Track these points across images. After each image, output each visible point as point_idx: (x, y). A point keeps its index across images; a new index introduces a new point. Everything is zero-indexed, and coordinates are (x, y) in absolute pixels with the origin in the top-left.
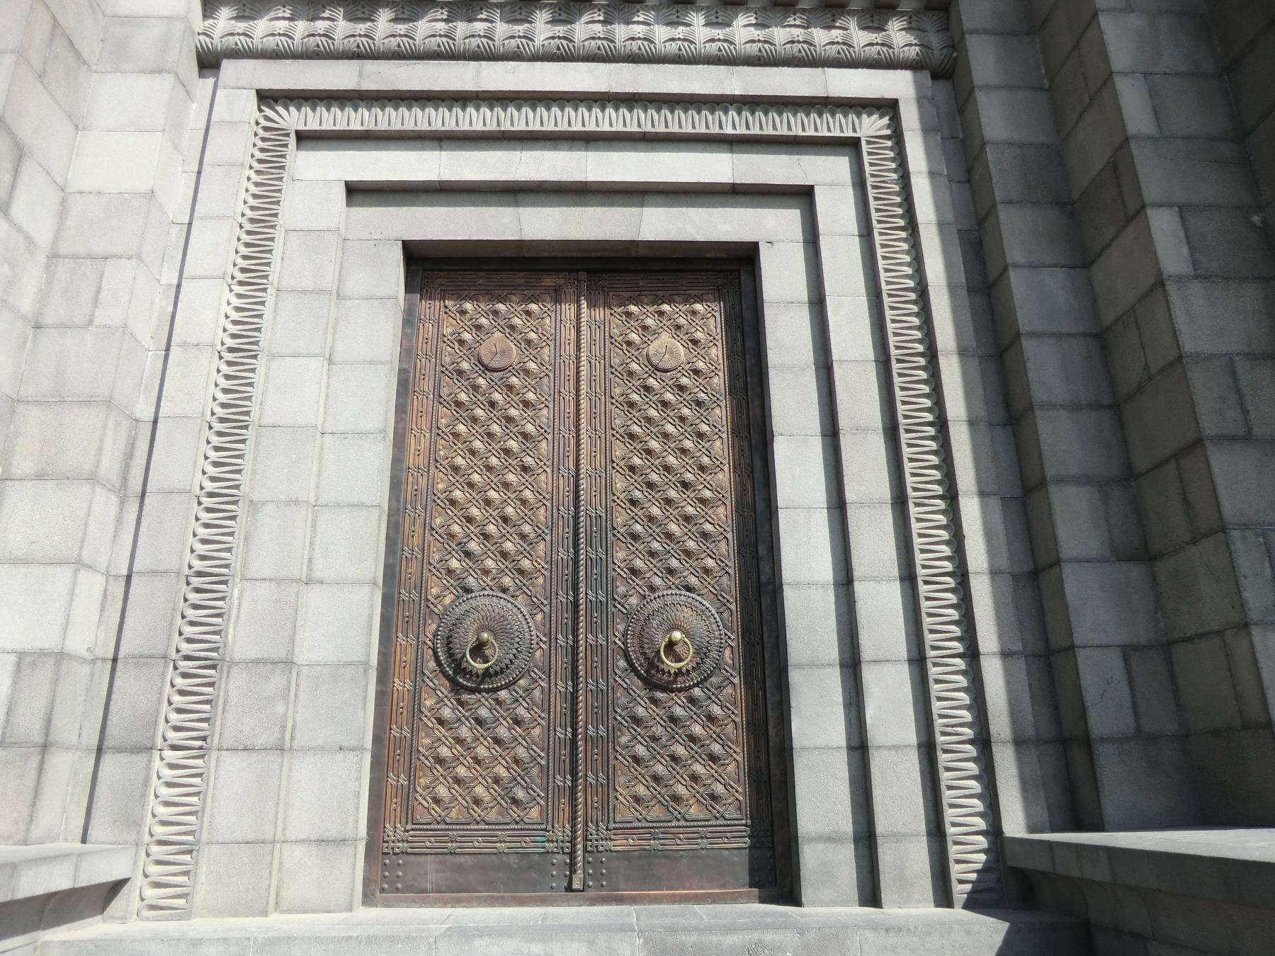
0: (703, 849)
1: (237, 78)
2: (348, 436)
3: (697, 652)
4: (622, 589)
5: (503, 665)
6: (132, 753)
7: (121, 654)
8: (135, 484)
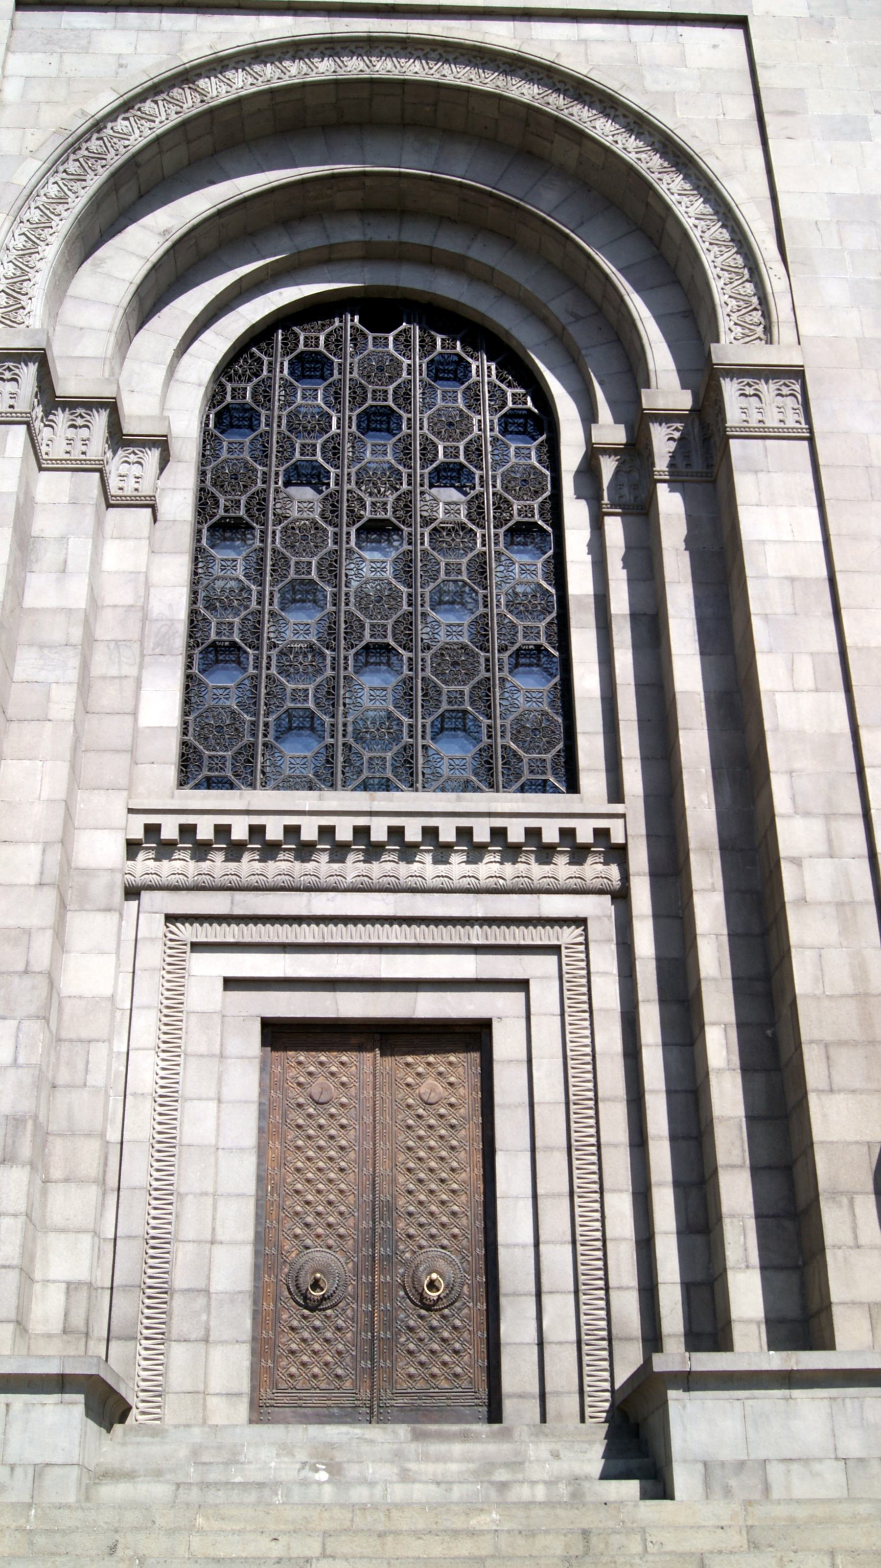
3: (446, 1287)
4: (402, 1247)
7: (115, 1284)
8: (112, 1181)
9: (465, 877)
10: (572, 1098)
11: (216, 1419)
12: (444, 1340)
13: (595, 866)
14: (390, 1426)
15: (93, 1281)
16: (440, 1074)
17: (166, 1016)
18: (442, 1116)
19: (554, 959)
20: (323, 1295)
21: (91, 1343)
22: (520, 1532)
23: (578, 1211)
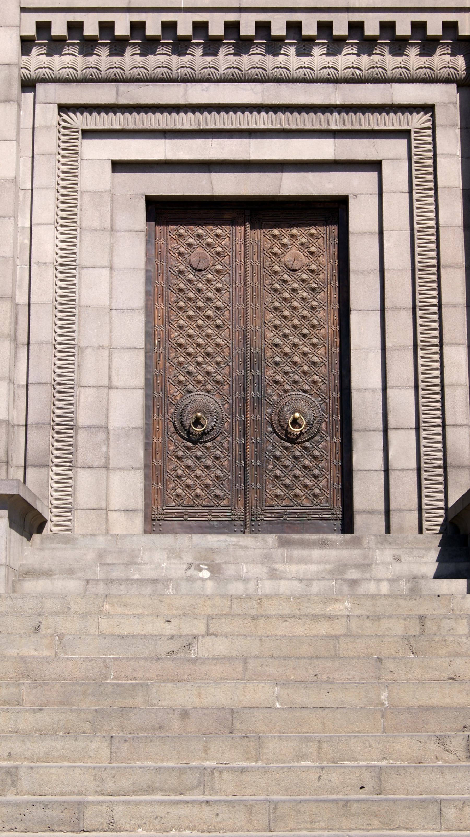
0: (309, 520)
1: (46, 97)
2: (125, 311)
3: (307, 424)
4: (270, 391)
5: (209, 430)
6: (40, 467)
7: (29, 422)
8: (23, 338)
9: (325, 68)
10: (417, 265)
11: (117, 530)
12: (305, 467)
13: (443, 57)
14: (260, 536)
15: (11, 419)
16: (302, 244)
17: (63, 195)
18: (304, 281)
19: (404, 142)
20: (204, 430)
21: (11, 470)
22: (368, 617)
23: (420, 361)
